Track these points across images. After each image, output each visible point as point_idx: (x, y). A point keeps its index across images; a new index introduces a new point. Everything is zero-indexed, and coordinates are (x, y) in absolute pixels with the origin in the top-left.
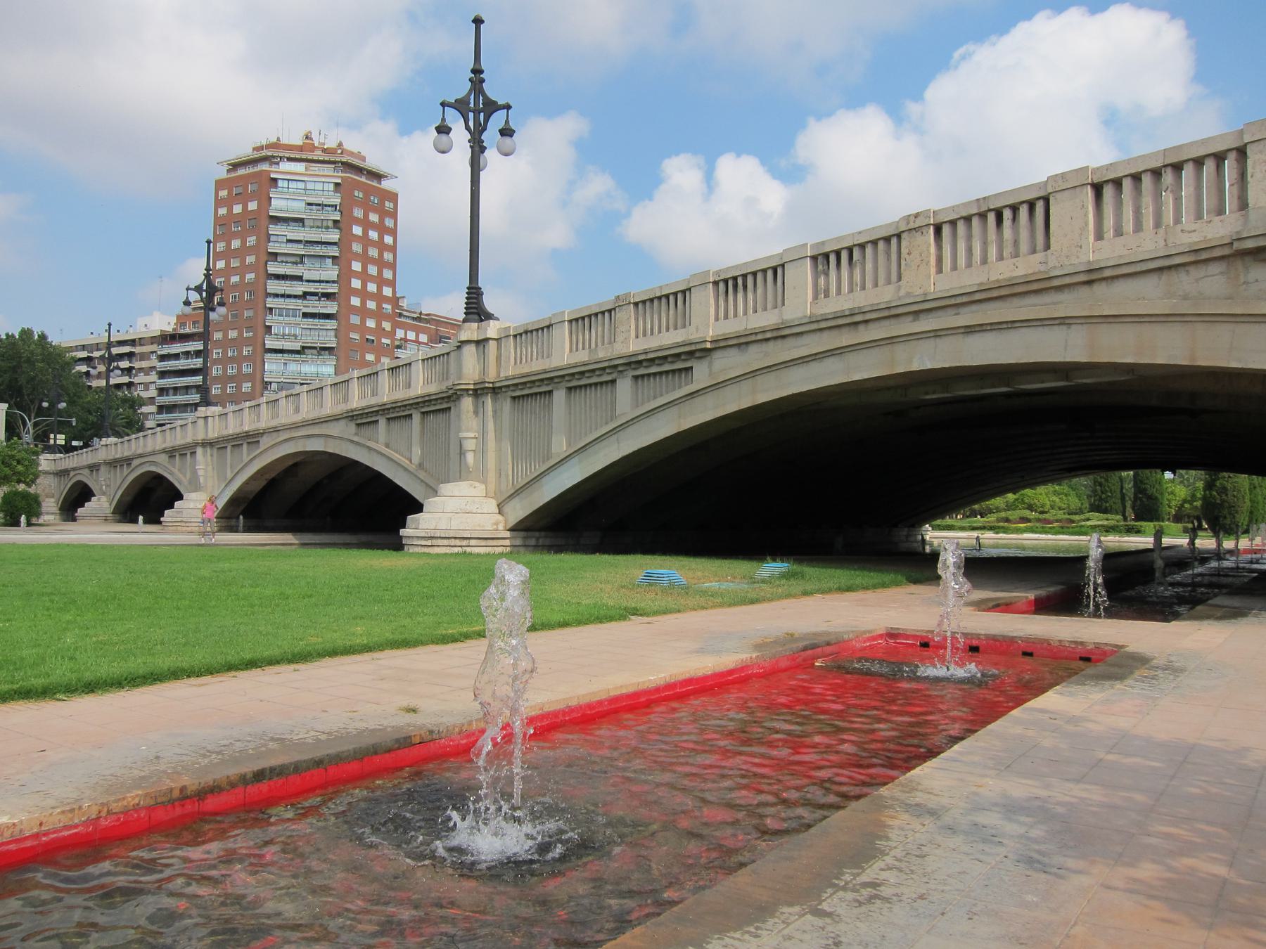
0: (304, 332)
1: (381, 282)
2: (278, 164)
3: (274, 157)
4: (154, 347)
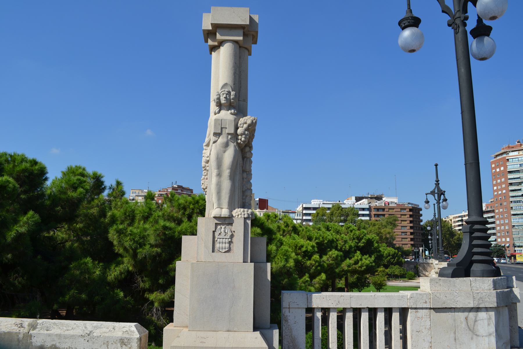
2: (509, 153)
3: (507, 152)
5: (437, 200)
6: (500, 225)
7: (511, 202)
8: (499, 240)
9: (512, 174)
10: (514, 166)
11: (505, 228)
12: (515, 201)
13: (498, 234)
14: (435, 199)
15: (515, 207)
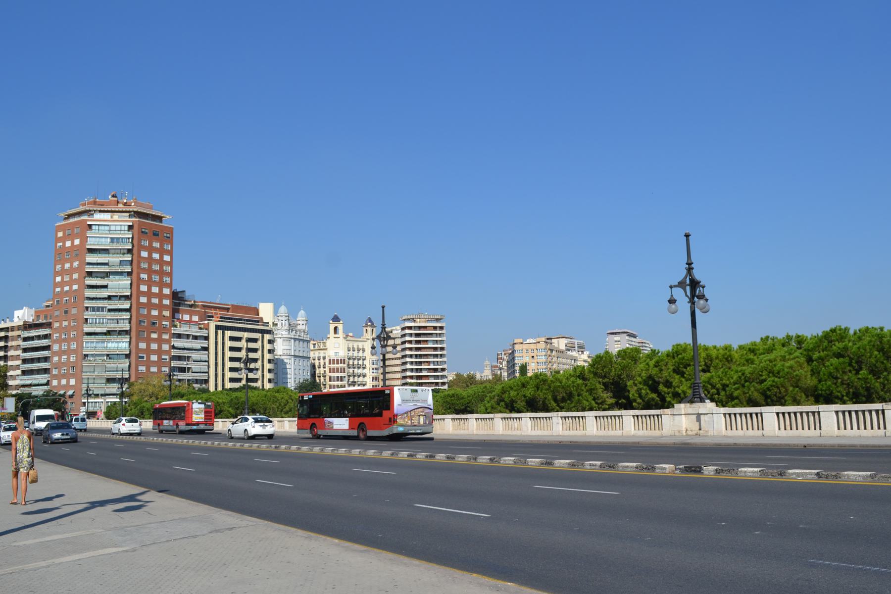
0: (109, 321)
1: (162, 285)
2: (93, 214)
3: (90, 211)
6: (60, 353)
7: (87, 308)
8: (55, 383)
9: (95, 255)
10: (101, 239)
11: (69, 358)
12: (93, 308)
13: (55, 372)
15: (92, 319)
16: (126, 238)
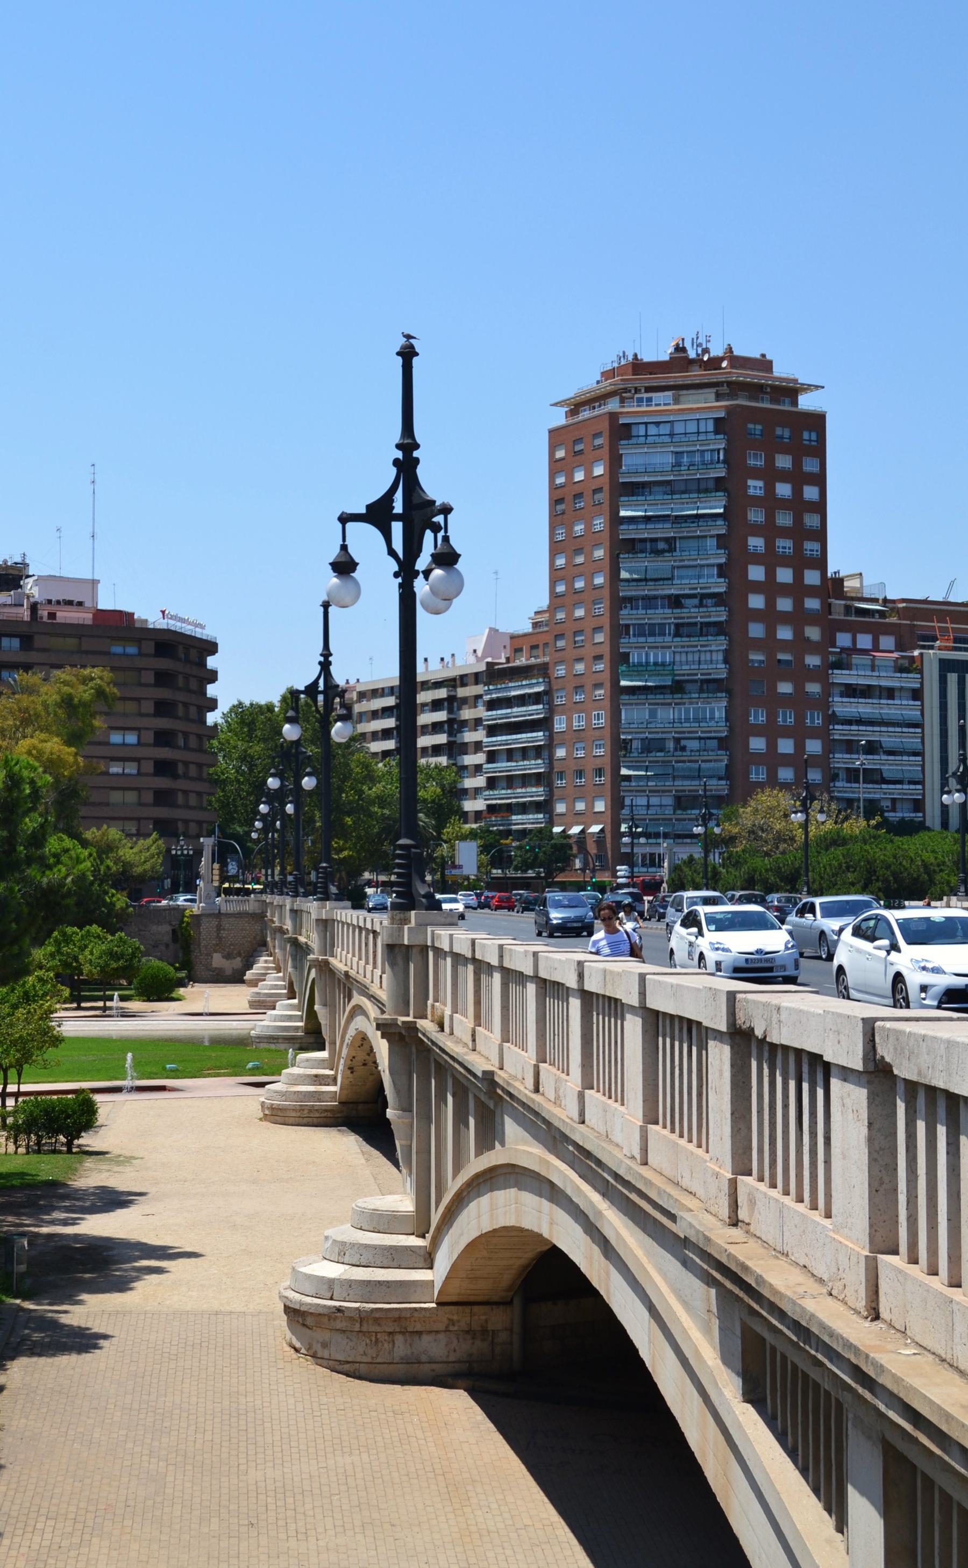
4: (479, 689)
5: (401, 555)
14: (392, 552)
16: (712, 451)
